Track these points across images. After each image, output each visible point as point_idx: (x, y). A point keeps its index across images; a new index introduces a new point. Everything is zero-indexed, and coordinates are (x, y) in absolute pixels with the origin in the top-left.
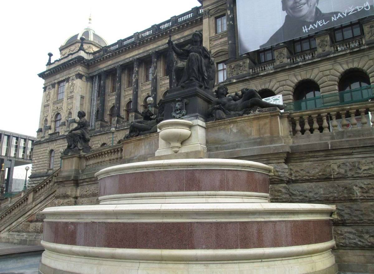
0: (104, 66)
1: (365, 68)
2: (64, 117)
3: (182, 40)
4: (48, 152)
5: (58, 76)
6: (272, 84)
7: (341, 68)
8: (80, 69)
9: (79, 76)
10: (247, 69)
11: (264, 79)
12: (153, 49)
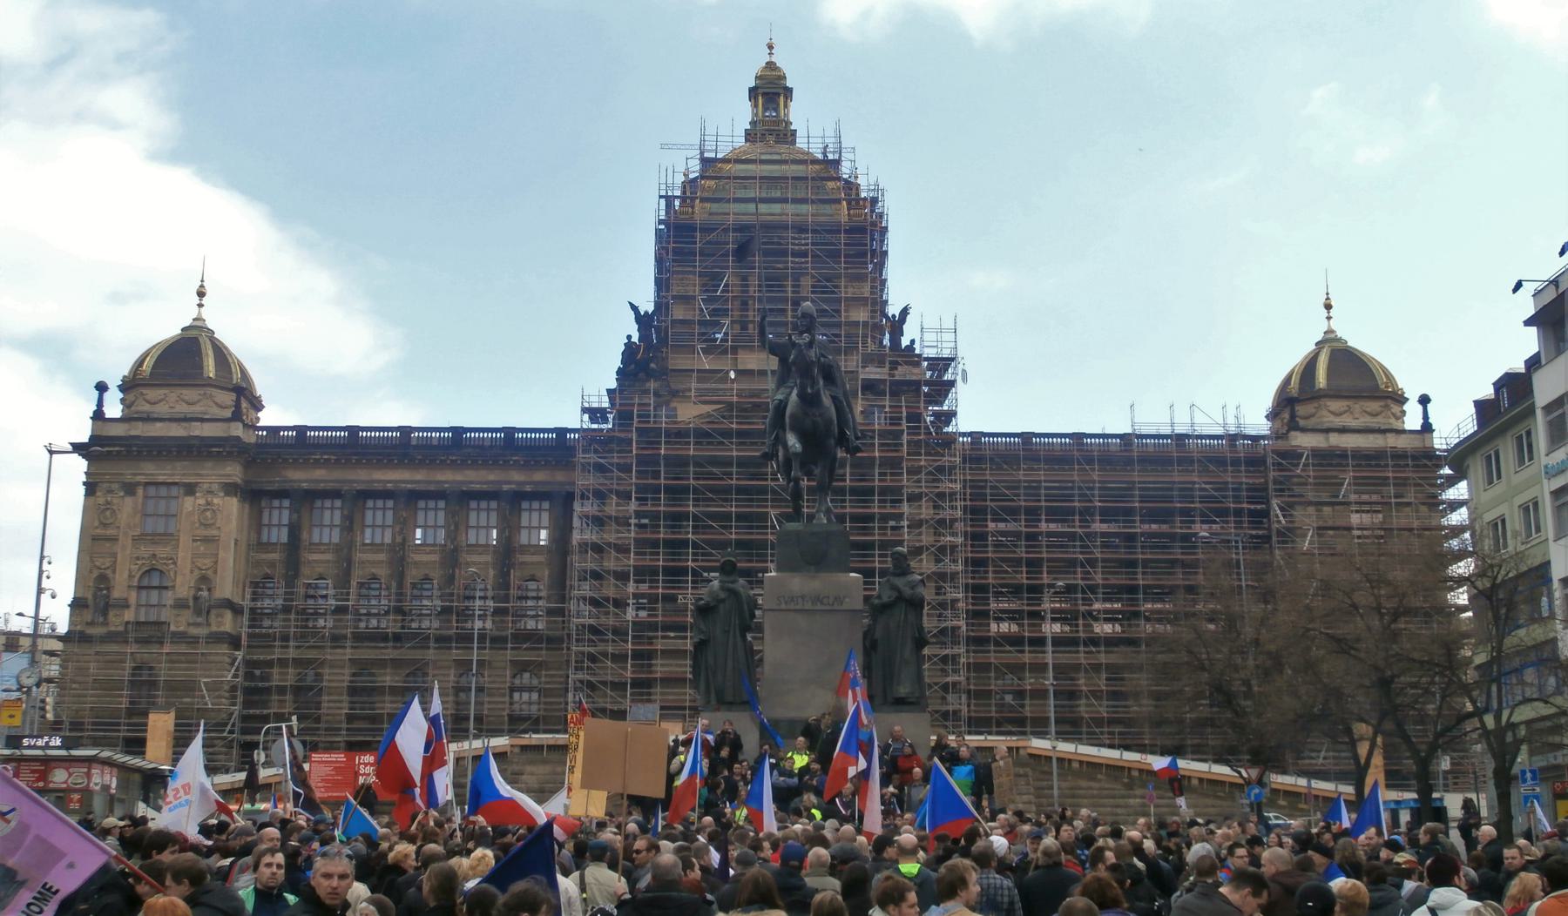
0: (300, 477)
3: (528, 488)
8: (234, 472)
9: (230, 489)
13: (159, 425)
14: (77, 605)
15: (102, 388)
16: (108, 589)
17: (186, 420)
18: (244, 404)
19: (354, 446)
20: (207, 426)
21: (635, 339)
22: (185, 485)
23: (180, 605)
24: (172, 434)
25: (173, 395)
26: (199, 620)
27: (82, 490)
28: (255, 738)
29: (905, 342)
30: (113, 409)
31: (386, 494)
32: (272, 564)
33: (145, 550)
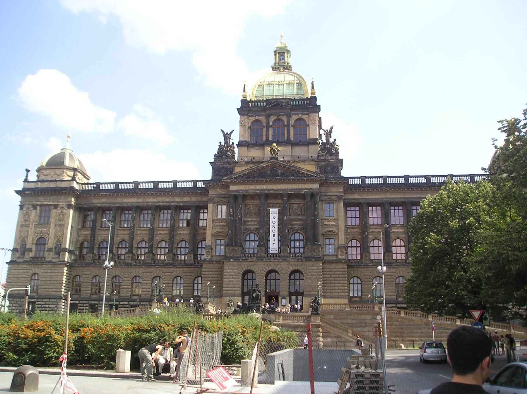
0: (98, 202)
1: (302, 271)
2: (51, 243)
3: (181, 204)
4: (30, 274)
5: (41, 199)
6: (254, 267)
7: (291, 268)
9: (69, 206)
10: (240, 253)
11: (250, 263)
12: (153, 202)
13: (46, 183)
14: (15, 250)
15: (28, 171)
16: (25, 245)
17: (56, 181)
18: (79, 177)
19: (117, 191)
20: (63, 183)
21: (223, 143)
22: (54, 205)
23: (50, 250)
24: (51, 187)
25: (52, 172)
26: (56, 256)
27: (18, 208)
28: (72, 302)
29: (332, 140)
30: (33, 177)
31: (129, 208)
32: (86, 235)
33: (39, 230)
